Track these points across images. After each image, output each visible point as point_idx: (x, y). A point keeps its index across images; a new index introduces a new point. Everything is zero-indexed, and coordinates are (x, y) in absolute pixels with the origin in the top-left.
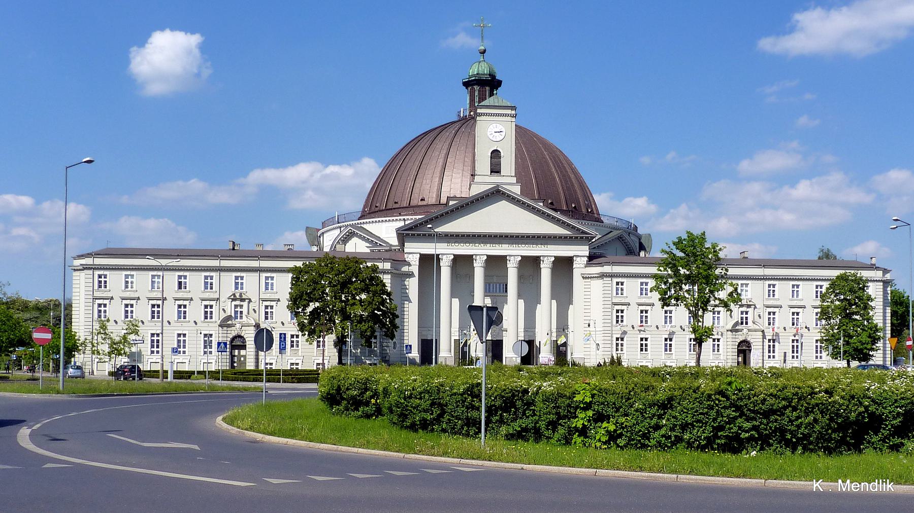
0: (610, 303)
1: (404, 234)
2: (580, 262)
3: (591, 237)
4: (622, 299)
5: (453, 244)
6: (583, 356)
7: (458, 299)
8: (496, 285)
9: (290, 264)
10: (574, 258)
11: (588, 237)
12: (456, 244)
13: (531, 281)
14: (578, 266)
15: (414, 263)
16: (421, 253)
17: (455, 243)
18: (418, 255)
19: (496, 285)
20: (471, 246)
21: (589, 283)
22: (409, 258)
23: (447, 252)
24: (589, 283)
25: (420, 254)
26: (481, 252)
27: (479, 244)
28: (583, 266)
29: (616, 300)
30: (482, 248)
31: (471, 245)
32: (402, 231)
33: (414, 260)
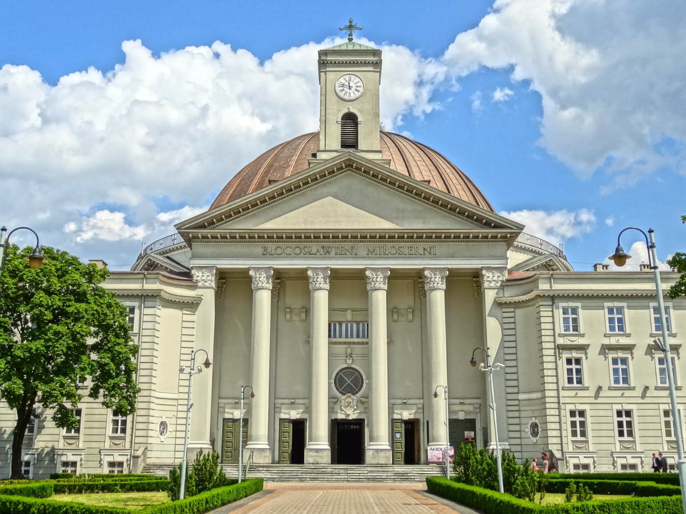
1: (189, 233)
2: (495, 278)
3: (510, 233)
8: (352, 327)
10: (484, 272)
13: (410, 316)
14: (492, 284)
15: (207, 284)
16: (219, 266)
19: (352, 327)
21: (512, 315)
22: (197, 274)
24: (512, 315)
25: (217, 269)
28: (499, 284)
29: (561, 341)
32: (186, 229)
33: (206, 280)
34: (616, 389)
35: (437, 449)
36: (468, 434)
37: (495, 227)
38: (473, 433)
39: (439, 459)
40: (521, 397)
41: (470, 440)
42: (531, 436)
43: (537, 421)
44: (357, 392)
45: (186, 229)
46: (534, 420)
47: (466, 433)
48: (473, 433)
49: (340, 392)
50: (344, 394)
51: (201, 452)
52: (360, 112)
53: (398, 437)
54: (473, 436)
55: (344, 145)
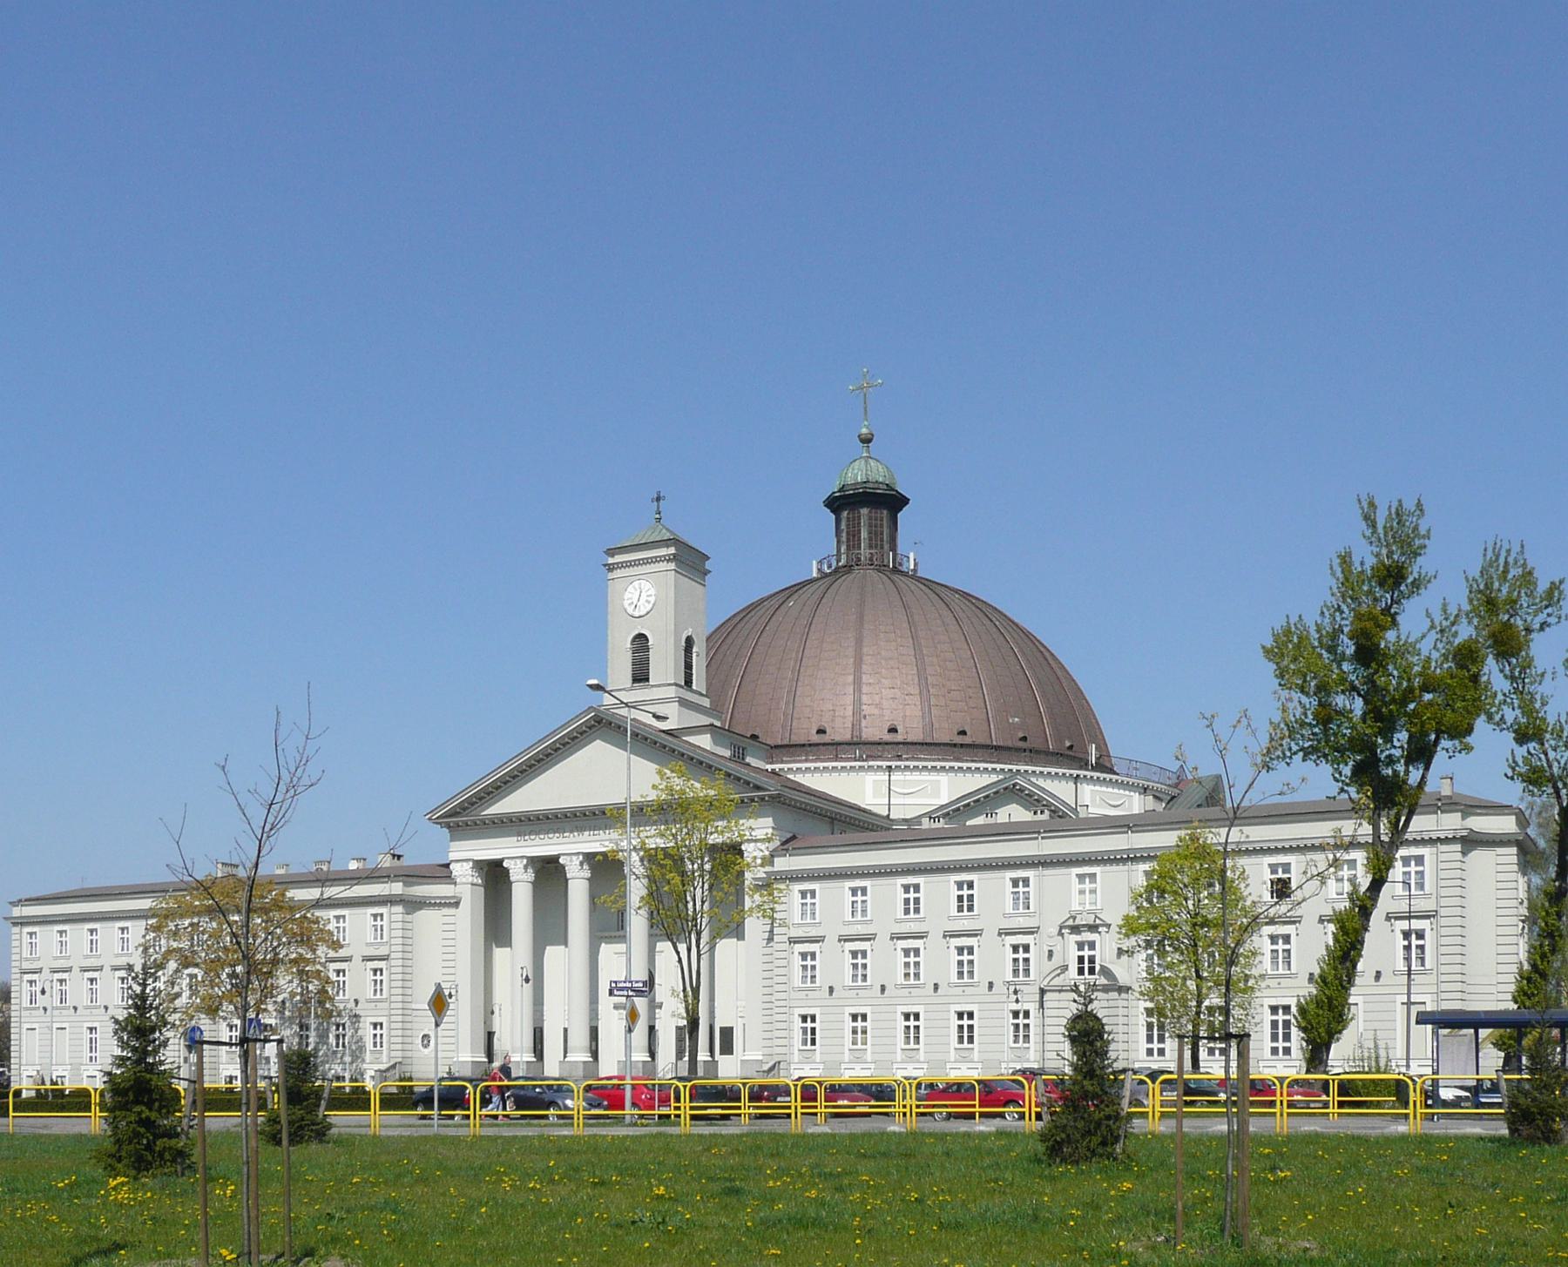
0: (785, 938)
4: (809, 929)
5: (527, 838)
6: (760, 1058)
7: (548, 948)
9: (145, 904)
11: (762, 799)
12: (532, 837)
15: (464, 880)
16: (476, 858)
17: (530, 834)
18: (471, 863)
20: (555, 838)
23: (514, 851)
26: (570, 848)
27: (571, 832)
30: (574, 840)
31: (557, 835)
33: (463, 872)
34: (904, 987)
45: (437, 818)
52: (653, 635)
55: (636, 680)
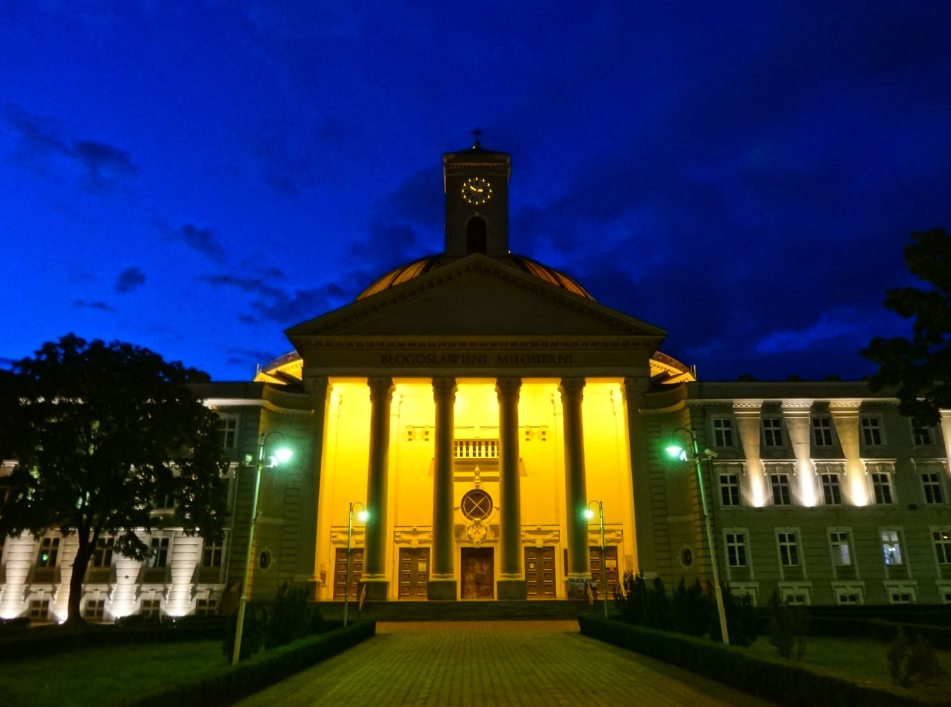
35: (578, 581)
36: (609, 563)
37: (637, 334)
38: (615, 561)
39: (580, 591)
40: (671, 519)
41: (612, 570)
42: (682, 565)
43: (690, 548)
44: (486, 517)
46: (686, 546)
47: (607, 562)
48: (615, 561)
49: (468, 517)
50: (471, 519)
51: (285, 587)
53: (532, 567)
54: (615, 566)
